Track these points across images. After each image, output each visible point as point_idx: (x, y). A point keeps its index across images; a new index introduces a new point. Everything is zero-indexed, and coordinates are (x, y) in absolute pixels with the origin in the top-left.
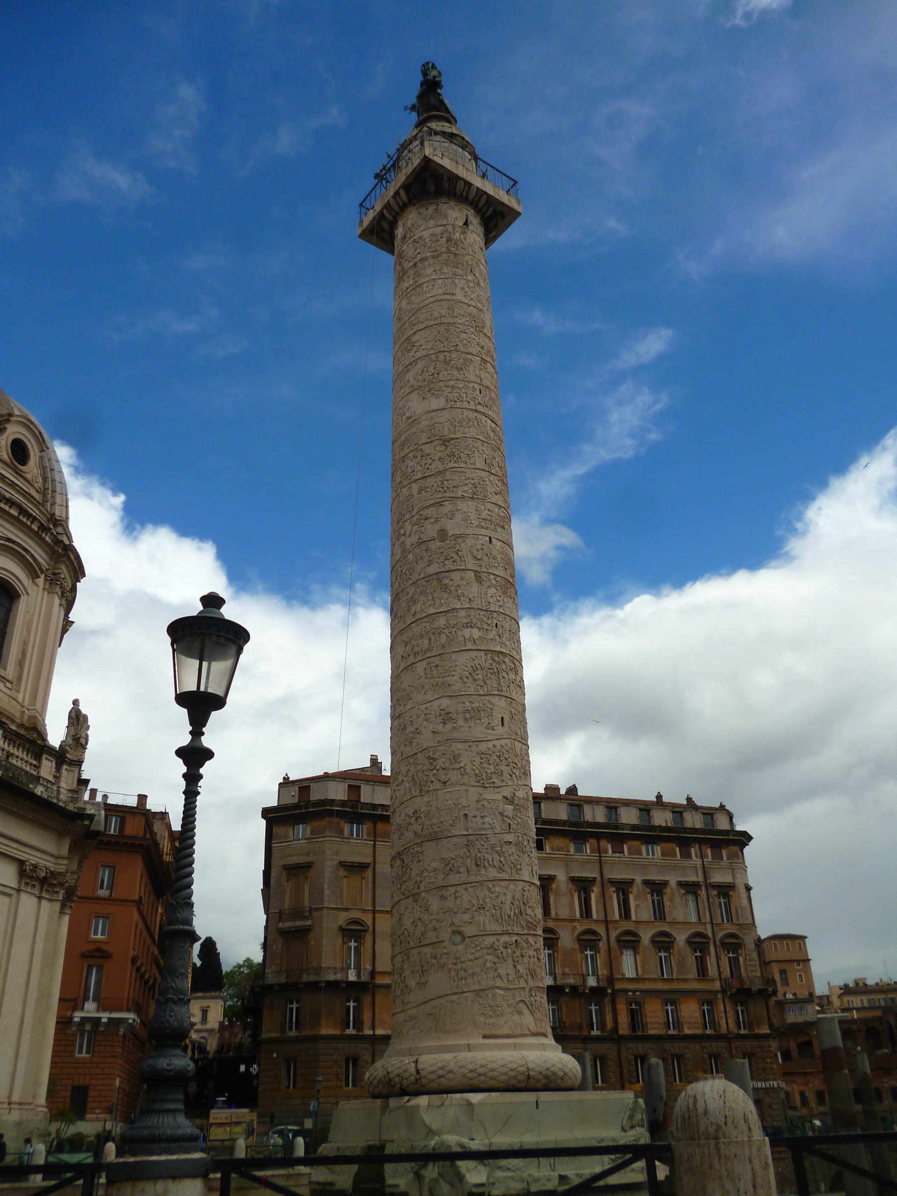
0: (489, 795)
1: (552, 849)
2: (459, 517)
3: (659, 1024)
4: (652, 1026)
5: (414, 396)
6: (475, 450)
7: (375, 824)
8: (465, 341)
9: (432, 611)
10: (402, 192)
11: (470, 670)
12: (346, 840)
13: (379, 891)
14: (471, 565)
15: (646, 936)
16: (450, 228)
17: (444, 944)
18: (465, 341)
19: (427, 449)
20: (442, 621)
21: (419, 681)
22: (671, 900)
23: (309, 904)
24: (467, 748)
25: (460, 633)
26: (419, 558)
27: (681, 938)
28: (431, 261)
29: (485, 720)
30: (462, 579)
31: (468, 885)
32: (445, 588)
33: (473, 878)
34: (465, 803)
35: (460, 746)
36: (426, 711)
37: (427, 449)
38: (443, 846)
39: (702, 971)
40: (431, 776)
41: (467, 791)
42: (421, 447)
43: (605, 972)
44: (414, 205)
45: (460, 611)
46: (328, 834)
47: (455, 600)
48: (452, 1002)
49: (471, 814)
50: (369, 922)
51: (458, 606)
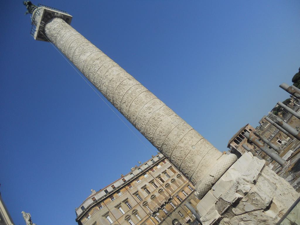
1: (141, 180)
2: (114, 71)
7: (103, 202)
9: (126, 91)
10: (43, 22)
11: (145, 96)
13: (114, 216)
14: (126, 78)
15: (170, 182)
17: (192, 150)
19: (94, 63)
20: (130, 92)
22: (169, 173)
25: (136, 91)
27: (175, 178)
29: (157, 104)
32: (125, 85)
34: (169, 121)
35: (157, 111)
37: (94, 63)
39: (183, 180)
41: (167, 119)
44: (47, 23)
47: (129, 86)
48: (204, 159)
50: (118, 223)
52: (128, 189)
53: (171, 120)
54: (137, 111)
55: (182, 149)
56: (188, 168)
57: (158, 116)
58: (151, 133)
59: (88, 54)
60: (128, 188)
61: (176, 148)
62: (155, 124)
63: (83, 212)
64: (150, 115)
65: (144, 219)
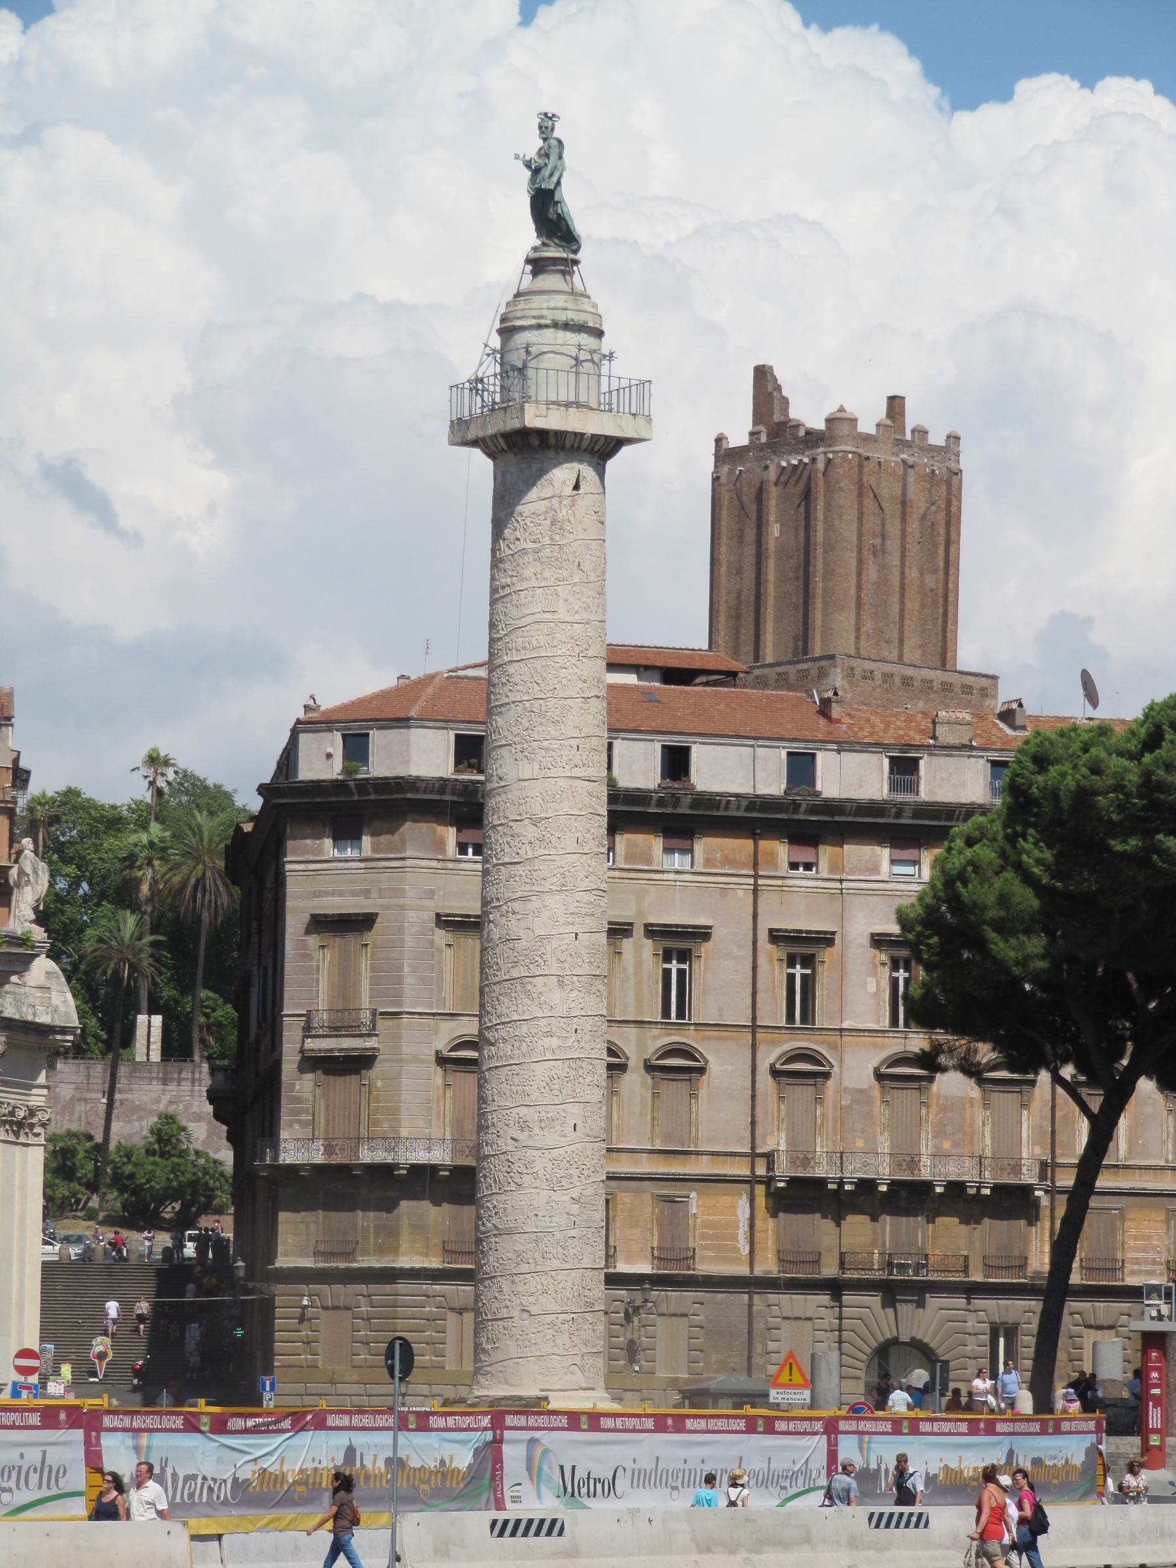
0: (556, 1197)
3: (1154, 1262)
4: (1136, 1267)
6: (566, 829)
8: (564, 681)
11: (548, 1080)
12: (450, 865)
16: (556, 506)
18: (564, 681)
20: (524, 1029)
23: (371, 1002)
30: (545, 985)
32: (528, 993)
33: (539, 1268)
35: (535, 1153)
42: (512, 824)
43: (1037, 1150)
46: (409, 853)
52: (776, 866)
54: (496, 1098)
59: (526, 770)
60: (772, 855)
63: (336, 786)
65: (703, 1167)
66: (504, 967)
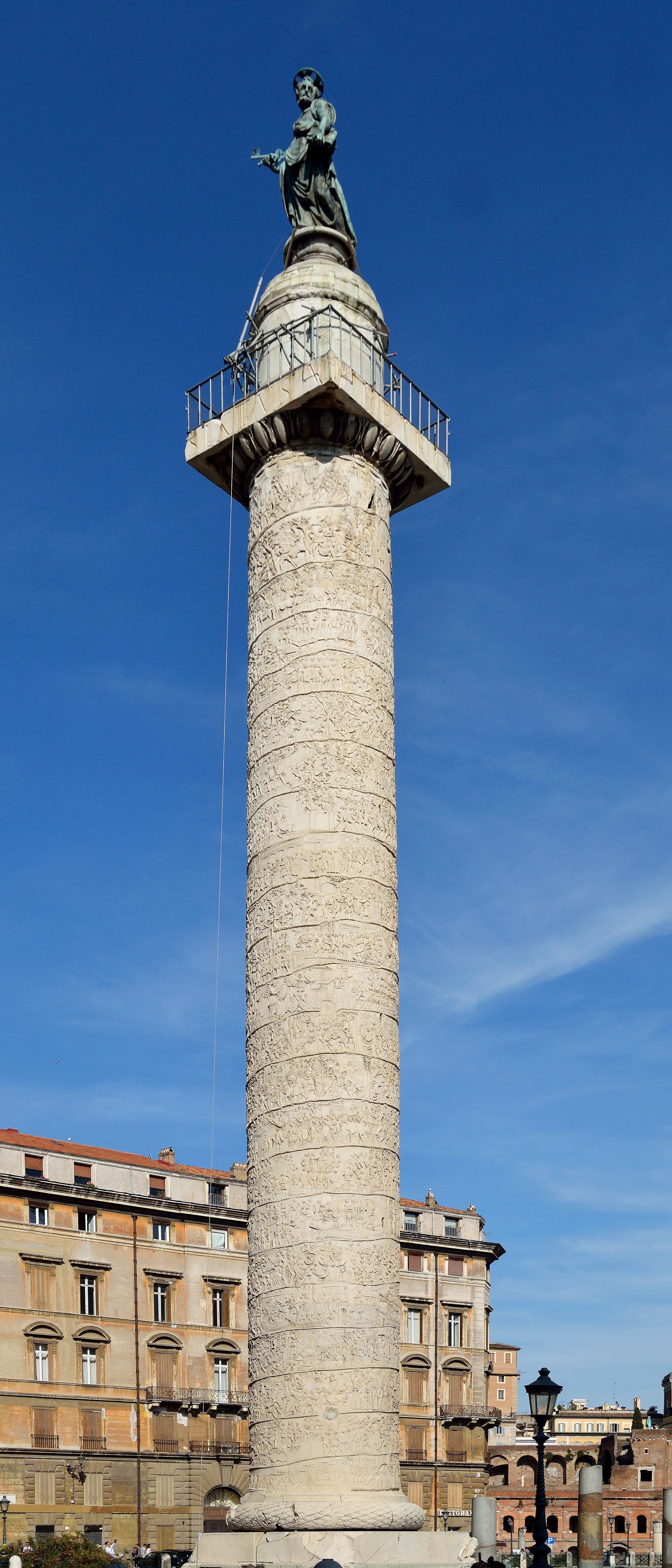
5: (290, 800)
9: (313, 1097)
20: (324, 1111)
21: (296, 1173)
24: (349, 1247)
25: (345, 1126)
26: (298, 1031)
28: (321, 571)
31: (343, 1371)
33: (348, 1365)
35: (340, 1244)
36: (303, 1205)
38: (320, 1336)
40: (308, 1270)
41: (345, 1288)
42: (303, 882)
45: (346, 1102)
49: (348, 1310)
51: (345, 1095)
53: (352, 1301)
55: (298, 1394)
56: (269, 1446)
57: (326, 1260)
58: (264, 1280)
61: (288, 1376)
62: (298, 1269)
64: (310, 1236)
66: (295, 1043)
